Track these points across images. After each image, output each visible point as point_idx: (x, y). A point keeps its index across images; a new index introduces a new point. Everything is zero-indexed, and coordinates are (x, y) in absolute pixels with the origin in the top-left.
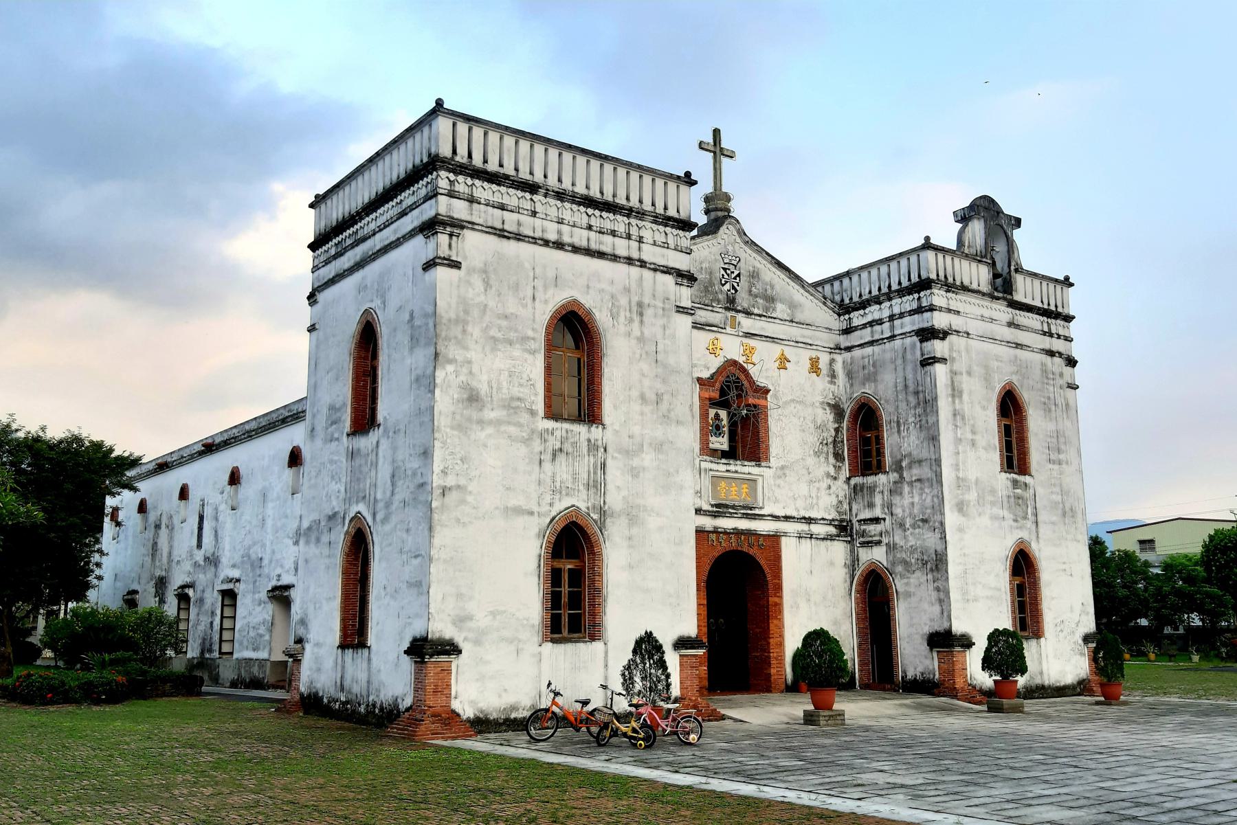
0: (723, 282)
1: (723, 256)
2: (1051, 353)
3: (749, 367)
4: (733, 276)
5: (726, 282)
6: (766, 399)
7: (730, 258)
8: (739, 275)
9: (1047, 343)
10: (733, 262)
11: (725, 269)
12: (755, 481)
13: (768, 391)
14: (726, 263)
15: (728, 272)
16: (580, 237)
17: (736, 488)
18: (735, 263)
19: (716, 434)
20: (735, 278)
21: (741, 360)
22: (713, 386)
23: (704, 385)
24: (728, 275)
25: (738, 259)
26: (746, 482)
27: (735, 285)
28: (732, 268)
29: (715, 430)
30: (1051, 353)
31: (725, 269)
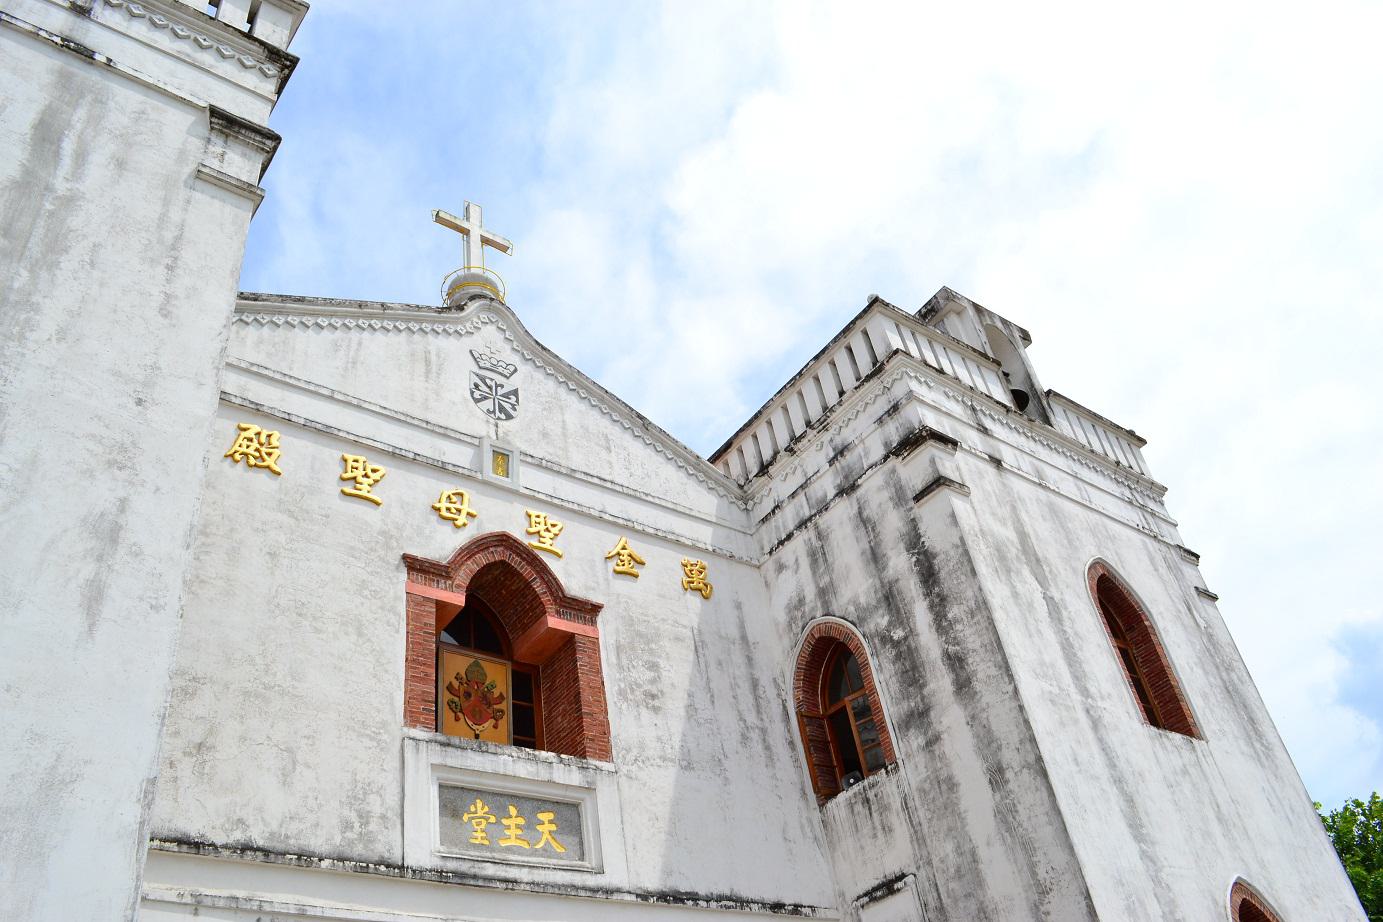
0: (477, 394)
6: (593, 623)
10: (500, 369)
13: (596, 609)
17: (521, 821)
18: (506, 372)
20: (505, 395)
22: (448, 577)
24: (490, 388)
25: (512, 369)
27: (507, 407)
28: (500, 379)
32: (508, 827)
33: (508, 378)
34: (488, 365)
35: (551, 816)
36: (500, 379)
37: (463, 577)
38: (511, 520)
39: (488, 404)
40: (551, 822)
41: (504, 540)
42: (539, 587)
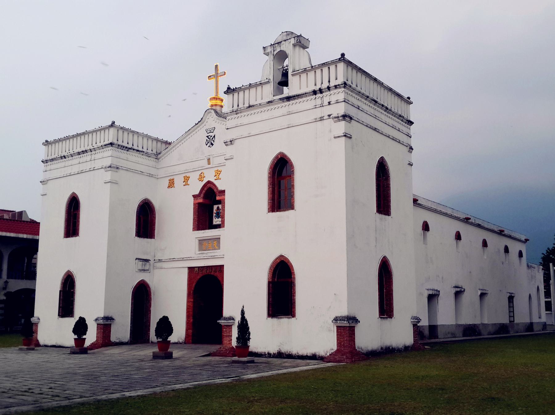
0: (207, 143)
1: (207, 130)
2: (322, 119)
3: (216, 183)
4: (208, 140)
5: (208, 143)
7: (210, 129)
8: (214, 137)
9: (318, 113)
10: (212, 131)
11: (207, 137)
12: (220, 238)
14: (208, 133)
15: (209, 137)
16: (76, 169)
18: (212, 131)
19: (217, 217)
20: (212, 139)
21: (212, 180)
23: (196, 197)
25: (214, 128)
26: (216, 239)
27: (212, 142)
28: (211, 134)
29: (216, 216)
30: (322, 119)
31: (207, 137)
32: (214, 243)
33: (213, 132)
34: (209, 132)
35: (216, 242)
36: (211, 134)
37: (202, 195)
38: (210, 176)
39: (209, 144)
40: (216, 243)
41: (209, 182)
42: (215, 190)
